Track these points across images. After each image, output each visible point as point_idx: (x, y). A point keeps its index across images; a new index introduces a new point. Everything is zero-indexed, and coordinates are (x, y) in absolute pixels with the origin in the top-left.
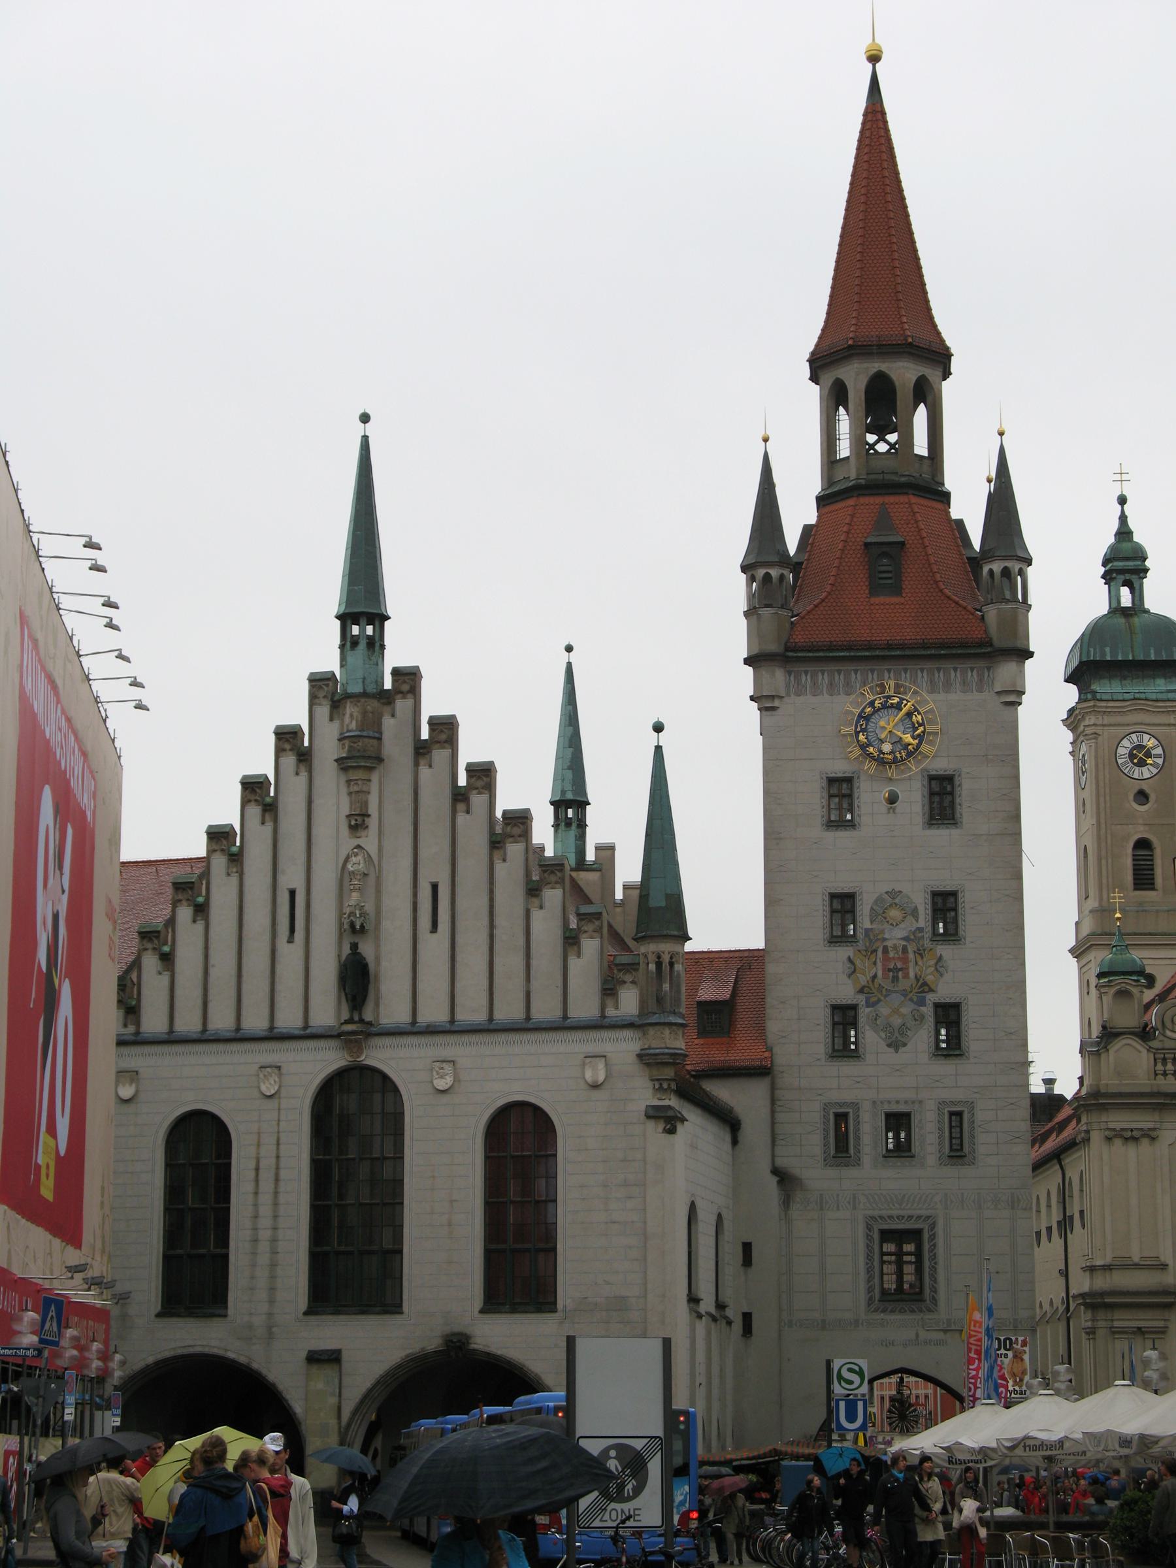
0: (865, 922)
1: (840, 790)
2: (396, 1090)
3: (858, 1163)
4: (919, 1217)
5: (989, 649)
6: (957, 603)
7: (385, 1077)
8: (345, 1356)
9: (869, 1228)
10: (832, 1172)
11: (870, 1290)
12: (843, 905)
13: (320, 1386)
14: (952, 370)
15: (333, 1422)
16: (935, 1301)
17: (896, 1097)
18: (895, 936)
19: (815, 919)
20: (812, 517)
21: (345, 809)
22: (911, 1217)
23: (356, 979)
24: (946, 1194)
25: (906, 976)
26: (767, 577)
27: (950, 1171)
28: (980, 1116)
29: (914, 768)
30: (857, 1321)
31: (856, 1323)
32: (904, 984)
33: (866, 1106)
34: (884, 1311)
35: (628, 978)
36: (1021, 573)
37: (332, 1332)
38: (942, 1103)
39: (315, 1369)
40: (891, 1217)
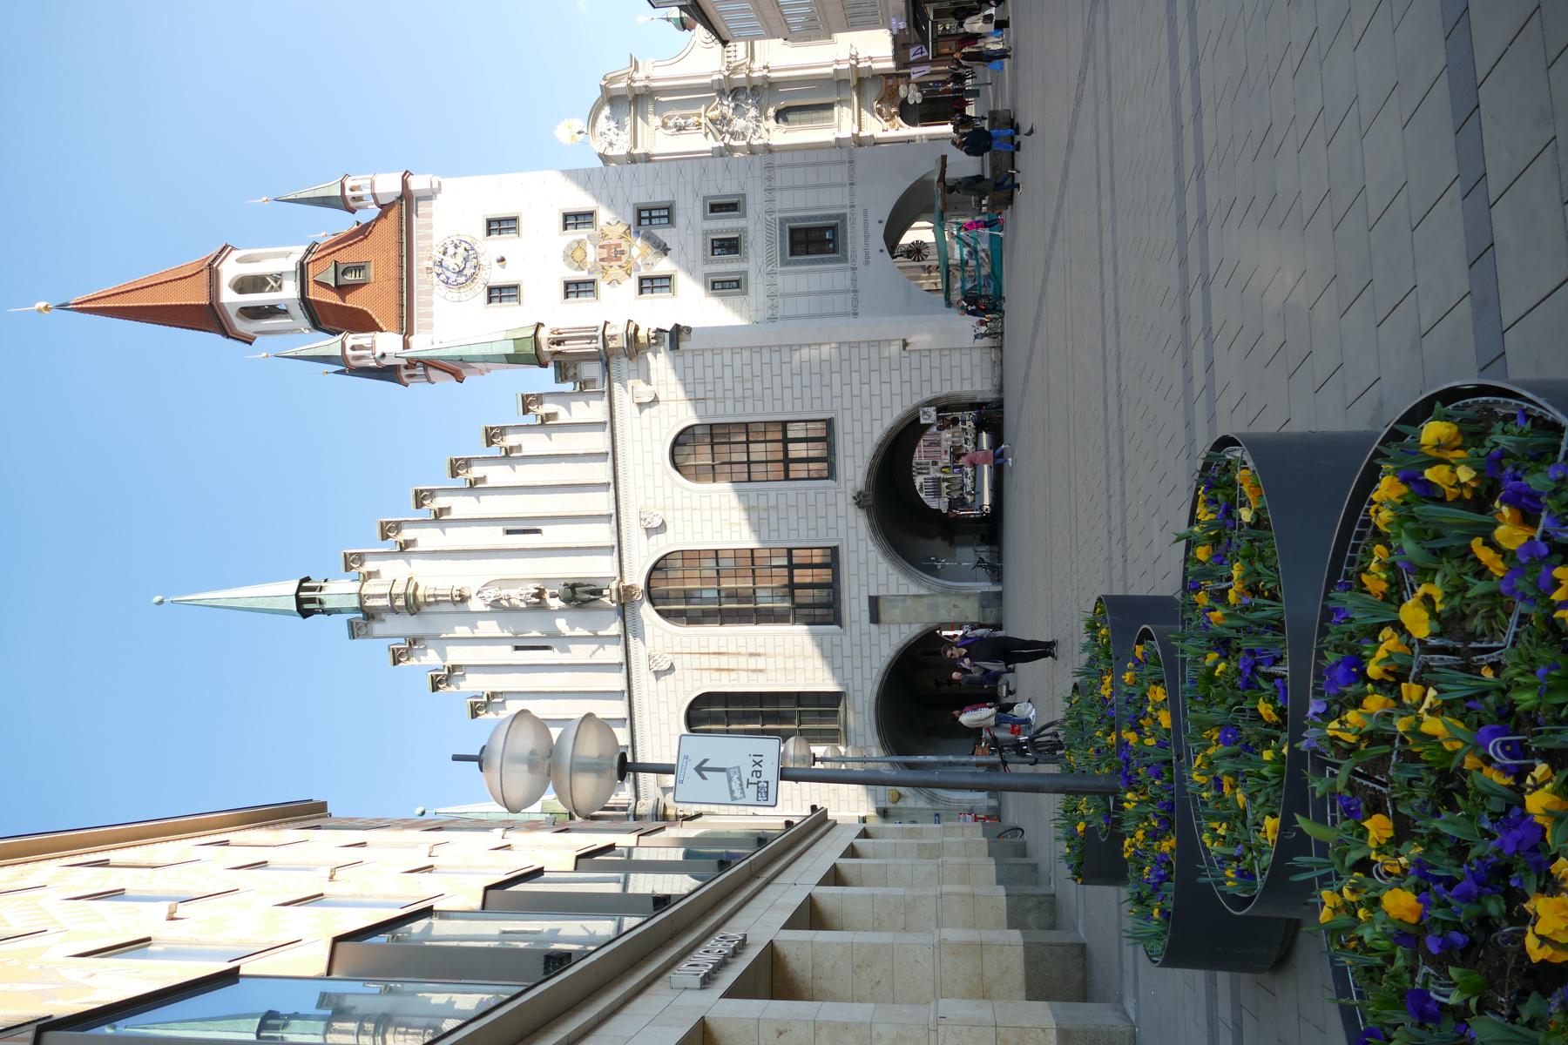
0: (582, 275)
1: (497, 293)
2: (664, 558)
3: (745, 273)
7: (655, 568)
8: (873, 593)
9: (789, 264)
10: (751, 288)
12: (573, 289)
13: (897, 612)
15: (926, 601)
16: (837, 216)
18: (592, 254)
21: (451, 608)
23: (580, 596)
25: (619, 245)
26: (353, 348)
27: (750, 210)
28: (714, 192)
29: (479, 248)
32: (624, 247)
34: (845, 250)
35: (571, 372)
37: (854, 606)
38: (705, 218)
39: (883, 617)
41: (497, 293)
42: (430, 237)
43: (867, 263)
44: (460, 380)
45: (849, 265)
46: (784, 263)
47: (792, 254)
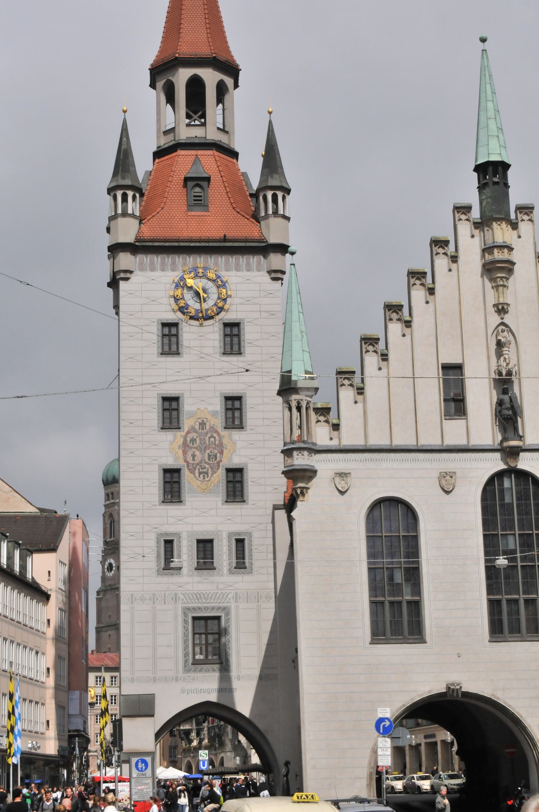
1: (170, 332)
4: (219, 608)
5: (264, 244)
6: (243, 216)
9: (185, 614)
11: (186, 655)
14: (239, 84)
17: (205, 529)
19: (153, 415)
20: (149, 166)
22: (213, 608)
24: (236, 593)
30: (177, 678)
31: (177, 679)
33: (184, 535)
34: (195, 671)
36: (284, 198)
40: (199, 608)
41: (170, 332)
42: (227, 270)
43: (183, 691)
44: (109, 285)
45: (181, 674)
46: (186, 611)
47: (194, 619)
